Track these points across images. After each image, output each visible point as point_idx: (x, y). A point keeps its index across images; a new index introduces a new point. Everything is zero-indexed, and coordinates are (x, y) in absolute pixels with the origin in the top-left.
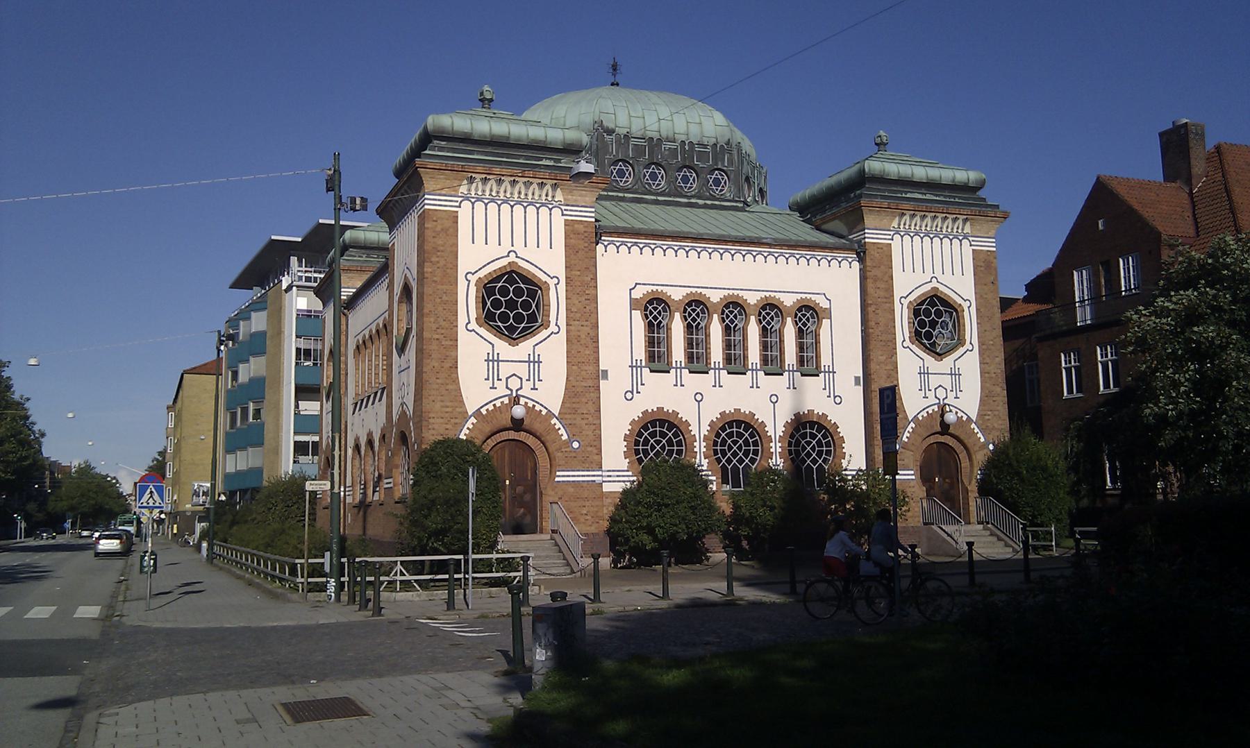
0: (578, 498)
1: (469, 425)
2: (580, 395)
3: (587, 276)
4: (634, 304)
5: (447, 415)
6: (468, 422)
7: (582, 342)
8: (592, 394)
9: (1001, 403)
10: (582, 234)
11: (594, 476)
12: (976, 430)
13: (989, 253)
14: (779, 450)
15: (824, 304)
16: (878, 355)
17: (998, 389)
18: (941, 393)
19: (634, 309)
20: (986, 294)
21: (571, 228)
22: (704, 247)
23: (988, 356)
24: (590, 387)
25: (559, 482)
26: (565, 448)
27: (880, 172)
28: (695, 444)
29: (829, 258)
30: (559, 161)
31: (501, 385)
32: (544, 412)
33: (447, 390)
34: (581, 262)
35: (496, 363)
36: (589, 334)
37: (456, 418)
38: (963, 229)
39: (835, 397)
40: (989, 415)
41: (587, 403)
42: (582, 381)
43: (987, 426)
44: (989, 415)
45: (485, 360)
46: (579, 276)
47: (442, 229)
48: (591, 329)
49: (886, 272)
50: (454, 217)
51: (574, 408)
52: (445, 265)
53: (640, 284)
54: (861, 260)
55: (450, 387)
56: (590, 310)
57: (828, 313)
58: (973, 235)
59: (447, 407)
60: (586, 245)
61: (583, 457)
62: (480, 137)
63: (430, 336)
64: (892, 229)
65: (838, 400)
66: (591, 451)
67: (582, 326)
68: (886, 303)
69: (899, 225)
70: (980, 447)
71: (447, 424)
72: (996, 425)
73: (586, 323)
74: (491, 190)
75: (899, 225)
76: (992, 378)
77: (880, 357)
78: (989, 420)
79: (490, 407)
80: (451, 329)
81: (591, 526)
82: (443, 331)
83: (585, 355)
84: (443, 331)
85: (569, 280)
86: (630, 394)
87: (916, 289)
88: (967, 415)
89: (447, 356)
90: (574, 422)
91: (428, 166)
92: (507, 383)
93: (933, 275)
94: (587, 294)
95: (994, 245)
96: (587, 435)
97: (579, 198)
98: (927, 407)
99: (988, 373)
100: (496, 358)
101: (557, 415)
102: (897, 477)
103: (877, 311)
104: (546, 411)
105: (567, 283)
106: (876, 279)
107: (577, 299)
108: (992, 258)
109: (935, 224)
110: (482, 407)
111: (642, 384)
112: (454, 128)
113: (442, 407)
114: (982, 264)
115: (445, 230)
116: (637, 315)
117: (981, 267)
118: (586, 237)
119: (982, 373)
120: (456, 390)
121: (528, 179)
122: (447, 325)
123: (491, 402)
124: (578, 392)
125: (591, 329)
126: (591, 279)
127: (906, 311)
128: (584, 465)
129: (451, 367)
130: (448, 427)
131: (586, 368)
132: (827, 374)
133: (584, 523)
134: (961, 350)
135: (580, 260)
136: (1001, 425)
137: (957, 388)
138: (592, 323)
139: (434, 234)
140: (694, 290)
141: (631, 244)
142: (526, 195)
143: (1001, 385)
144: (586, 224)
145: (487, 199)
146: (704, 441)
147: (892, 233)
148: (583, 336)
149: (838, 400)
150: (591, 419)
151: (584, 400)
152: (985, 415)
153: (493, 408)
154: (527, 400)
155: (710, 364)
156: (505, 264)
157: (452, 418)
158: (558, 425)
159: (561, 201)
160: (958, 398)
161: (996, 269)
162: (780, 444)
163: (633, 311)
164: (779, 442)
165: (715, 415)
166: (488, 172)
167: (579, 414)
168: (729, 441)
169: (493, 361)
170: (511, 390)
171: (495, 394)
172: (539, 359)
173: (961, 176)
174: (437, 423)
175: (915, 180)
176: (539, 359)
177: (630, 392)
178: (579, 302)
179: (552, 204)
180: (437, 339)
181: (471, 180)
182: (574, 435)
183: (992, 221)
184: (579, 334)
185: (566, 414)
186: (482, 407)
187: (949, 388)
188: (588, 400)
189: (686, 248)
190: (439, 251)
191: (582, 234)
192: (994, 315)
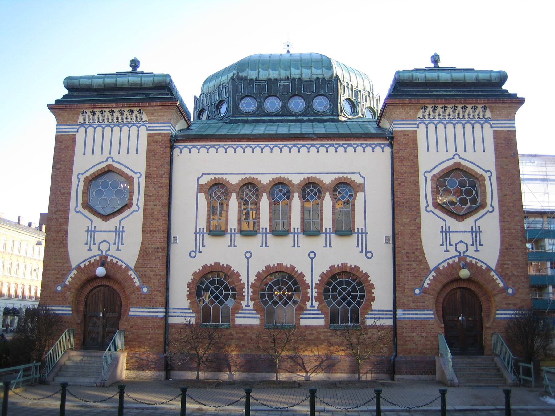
7: (155, 216)
8: (160, 254)
14: (315, 294)
24: (158, 248)
31: (452, 249)
35: (448, 234)
36: (160, 211)
42: (153, 245)
67: (155, 205)
73: (158, 204)
82: (60, 213)
83: (156, 226)
86: (193, 254)
89: (62, 229)
111: (122, 244)
122: (62, 209)
146: (251, 288)
151: (153, 258)
155: (259, 230)
162: (316, 290)
164: (315, 288)
165: (325, 269)
170: (460, 253)
171: (448, 255)
172: (479, 229)
176: (479, 229)
180: (56, 218)
184: (153, 211)
188: (157, 258)
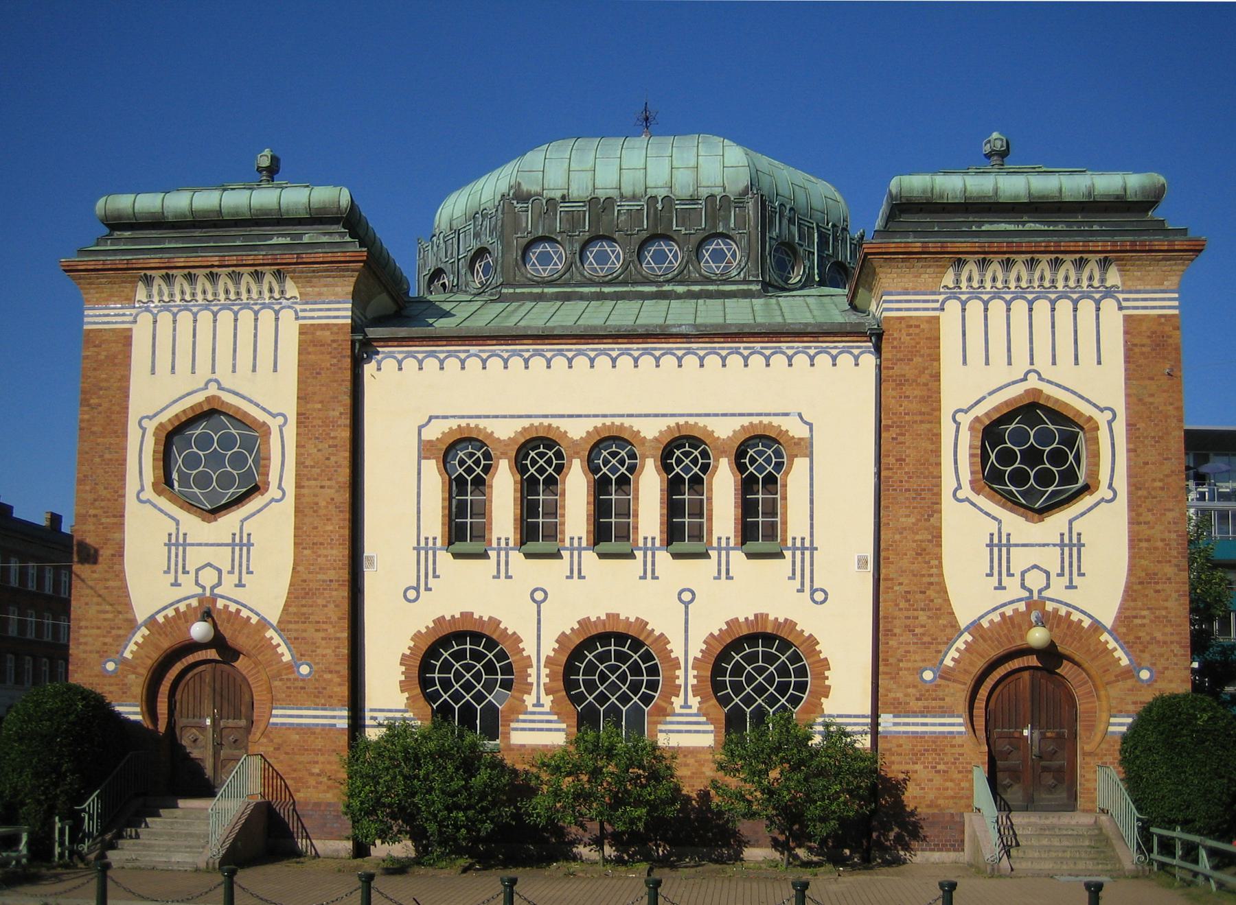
0: (307, 750)
1: (138, 638)
2: (313, 594)
3: (334, 410)
4: (425, 449)
5: (106, 624)
6: (136, 635)
7: (322, 512)
8: (334, 593)
9: (1175, 595)
10: (330, 345)
11: (334, 717)
12: (1112, 644)
13: (1163, 320)
14: (692, 681)
15: (797, 430)
16: (902, 517)
17: (1169, 570)
18: (1035, 581)
19: (426, 458)
20: (1152, 395)
21: (309, 337)
22: (558, 350)
23: (1149, 510)
24: (331, 581)
25: (277, 724)
26: (286, 674)
27: (924, 191)
28: (529, 671)
29: (636, 354)
30: (300, 236)
31: (1012, 584)
32: (254, 619)
33: (107, 588)
34: (324, 389)
35: (1004, 550)
36: (332, 499)
37: (119, 628)
38: (1103, 280)
39: (813, 591)
40: (1144, 617)
41: (325, 606)
42: (317, 573)
43: (1139, 638)
44: (1144, 617)
45: (165, 544)
46: (319, 410)
47: (107, 357)
48: (337, 491)
49: (925, 368)
50: (126, 339)
51: (304, 614)
52: (109, 409)
53: (437, 417)
54: (878, 350)
55: (111, 583)
56: (336, 463)
57: (805, 447)
58: (1126, 288)
59: (107, 612)
60: (335, 361)
61: (316, 688)
62: (176, 217)
63: (84, 511)
64: (942, 290)
65: (819, 596)
66: (331, 681)
67: (322, 487)
68: (922, 422)
69: (958, 281)
70: (1116, 676)
71: (104, 636)
72: (1158, 635)
73: (327, 483)
74: (183, 293)
75: (958, 281)
76: (1156, 548)
77: (903, 520)
78: (1143, 625)
79: (171, 612)
80: (116, 500)
81: (324, 792)
82: (103, 504)
83: (325, 532)
84: (103, 504)
85: (302, 419)
86: (413, 593)
87: (990, 394)
88: (1090, 616)
89: (109, 540)
90: (304, 635)
91: (80, 268)
92: (197, 577)
93: (1032, 367)
94: (333, 438)
95: (1176, 303)
96: (324, 656)
97: (325, 289)
98: (178, 601)
99: (1148, 540)
100: (181, 541)
101: (275, 623)
102: (273, 720)
103: (901, 439)
104: (258, 618)
105: (299, 423)
106: (901, 382)
107: (315, 447)
108: (1168, 329)
109: (1037, 275)
110: (159, 612)
112: (136, 211)
113: (99, 612)
114: (1147, 341)
115: (111, 358)
116: (431, 468)
117: (1143, 345)
118: (335, 349)
119: (1134, 542)
120: (120, 588)
121: (232, 269)
122: (109, 496)
123: (171, 605)
124: (310, 590)
125: (337, 491)
126: (341, 414)
127: (965, 438)
128: (317, 700)
129: (113, 555)
130: (108, 640)
131: (324, 552)
132: (798, 553)
133: (314, 787)
134: (1087, 501)
135: (323, 385)
136: (1172, 634)
137: (241, 568)
138: (338, 483)
139: (95, 365)
140: (756, 420)
141: (596, 353)
142: (238, 293)
143: (1174, 561)
144: (335, 329)
145: (175, 306)
146: (545, 667)
147: (941, 298)
148: (323, 504)
149: (819, 596)
150: (331, 630)
151: (320, 601)
152: (1135, 617)
153: (174, 613)
154: (228, 603)
155: (564, 541)
156: (201, 400)
157: (113, 628)
158: (277, 640)
159: (295, 298)
160: (180, 585)
161: (1177, 349)
162: (695, 672)
163: (423, 461)
164: (693, 668)
165: (716, 625)
166: (167, 265)
167: (309, 622)
168: (624, 667)
169: (177, 545)
170: (1031, 591)
171: (1003, 597)
172: (1079, 540)
173: (1107, 183)
174: (91, 636)
175: (1000, 201)
176: (1079, 540)
177: (413, 588)
178: (319, 450)
179: (281, 303)
180: (95, 516)
181: (148, 281)
182: (302, 655)
183: (1164, 259)
184: (316, 499)
185: (290, 622)
186: (159, 612)
187: (226, 567)
188: (329, 602)
189: (853, 351)
190: (101, 389)
191: (330, 345)
192: (1168, 434)
